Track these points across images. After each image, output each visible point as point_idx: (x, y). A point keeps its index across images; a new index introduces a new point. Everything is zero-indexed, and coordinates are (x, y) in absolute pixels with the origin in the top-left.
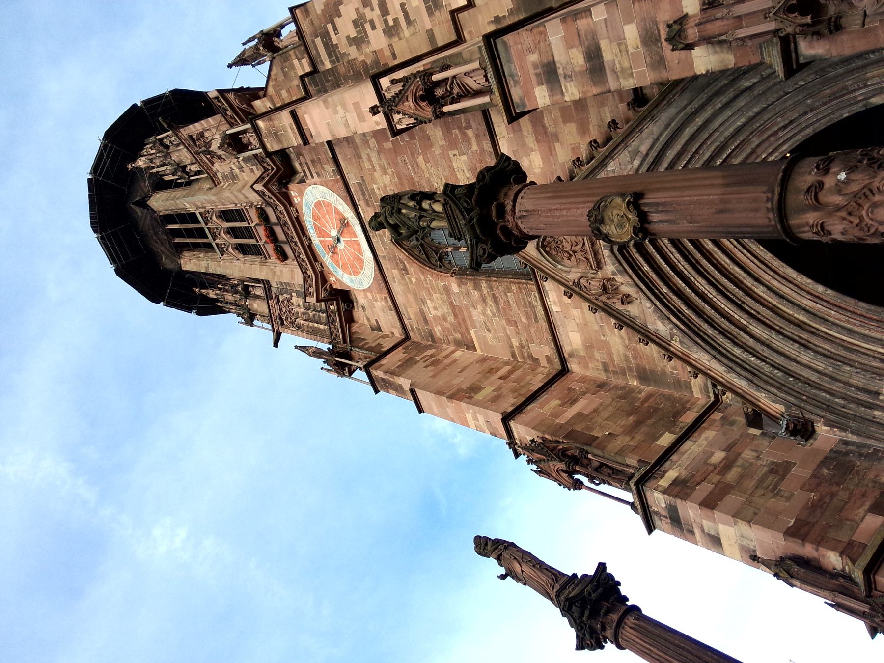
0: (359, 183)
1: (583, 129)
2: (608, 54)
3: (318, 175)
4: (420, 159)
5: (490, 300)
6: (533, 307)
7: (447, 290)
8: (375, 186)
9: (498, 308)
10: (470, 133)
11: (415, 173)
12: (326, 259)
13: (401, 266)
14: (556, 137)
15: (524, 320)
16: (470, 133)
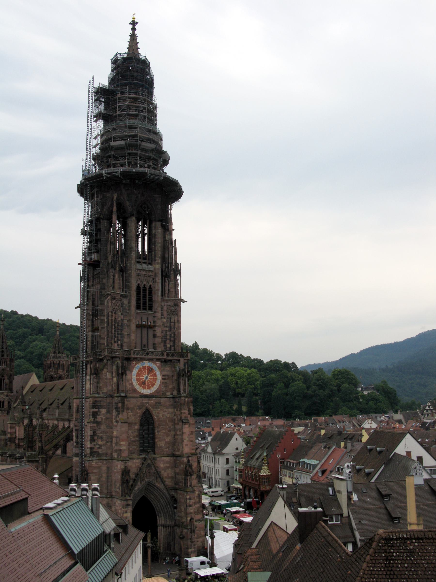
0: (160, 403)
1: (166, 477)
2: (191, 508)
3: (163, 382)
4: (164, 431)
5: (134, 439)
6: (134, 453)
7: (135, 424)
8: (159, 409)
9: (132, 441)
10: (167, 449)
11: (162, 427)
12: (140, 365)
13: (141, 407)
14: (165, 471)
15: (131, 449)
16: (167, 449)
